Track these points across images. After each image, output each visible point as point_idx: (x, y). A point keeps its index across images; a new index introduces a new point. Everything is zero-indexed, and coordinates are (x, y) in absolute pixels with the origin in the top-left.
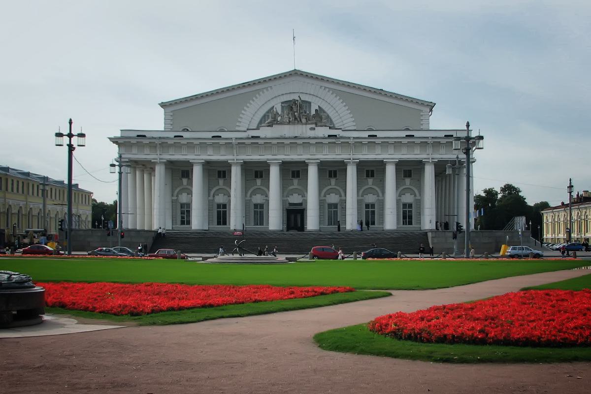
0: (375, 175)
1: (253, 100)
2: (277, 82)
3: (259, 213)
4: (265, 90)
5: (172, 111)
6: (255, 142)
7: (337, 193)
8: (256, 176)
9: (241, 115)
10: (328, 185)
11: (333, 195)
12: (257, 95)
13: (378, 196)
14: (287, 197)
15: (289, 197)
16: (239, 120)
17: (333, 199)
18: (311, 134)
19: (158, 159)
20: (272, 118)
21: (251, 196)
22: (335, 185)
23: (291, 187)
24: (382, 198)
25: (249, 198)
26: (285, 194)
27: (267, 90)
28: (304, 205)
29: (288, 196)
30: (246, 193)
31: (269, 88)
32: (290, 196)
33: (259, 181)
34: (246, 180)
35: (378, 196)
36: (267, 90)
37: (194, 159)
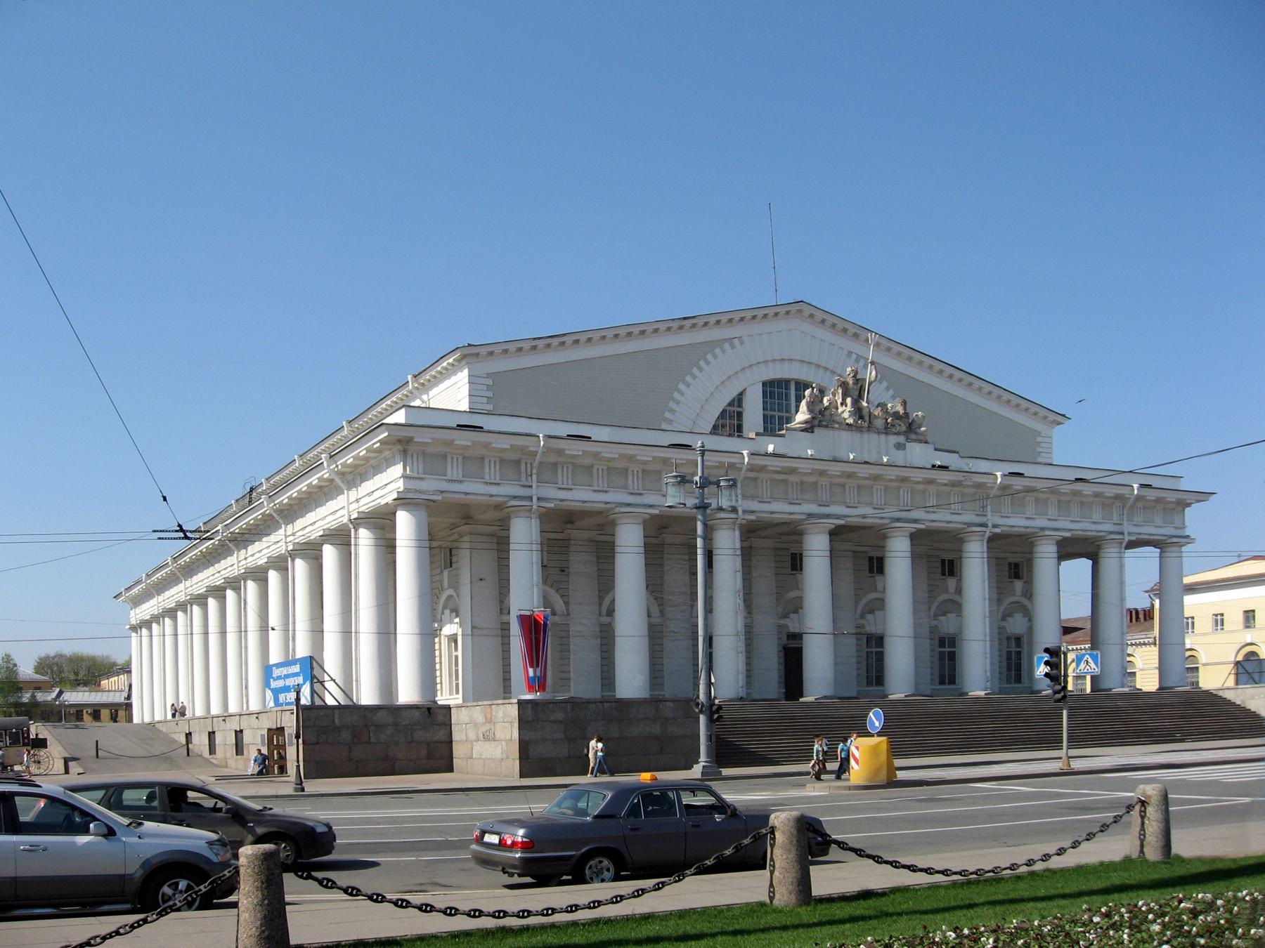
2: (755, 328)
4: (727, 346)
5: (489, 376)
16: (667, 415)
18: (899, 457)
19: (535, 499)
20: (810, 410)
27: (733, 347)
31: (736, 342)
36: (733, 347)
37: (628, 505)
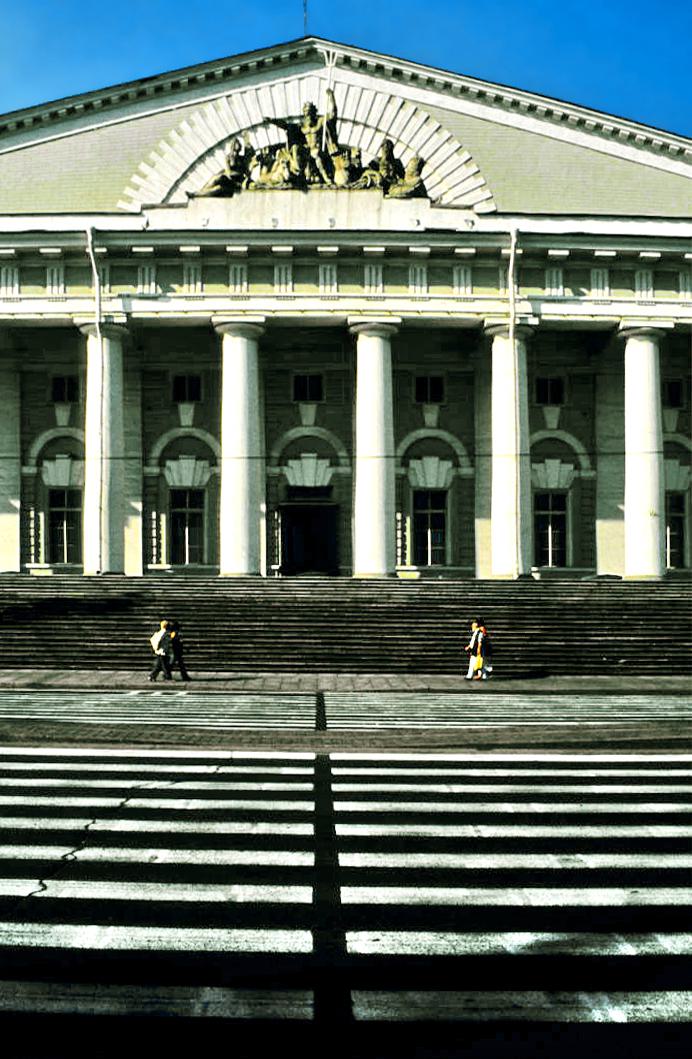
0: (566, 396)
1: (169, 142)
3: (189, 515)
6: (168, 260)
7: (446, 453)
8: (179, 397)
9: (128, 191)
10: (416, 428)
11: (431, 463)
12: (184, 125)
13: (578, 467)
14: (279, 465)
15: (286, 465)
17: (432, 473)
21: (161, 464)
22: (439, 427)
23: (294, 433)
24: (592, 474)
25: (156, 470)
26: (276, 454)
28: (336, 491)
29: (283, 461)
30: (146, 449)
32: (291, 462)
33: (187, 413)
34: (146, 407)
35: (578, 467)
